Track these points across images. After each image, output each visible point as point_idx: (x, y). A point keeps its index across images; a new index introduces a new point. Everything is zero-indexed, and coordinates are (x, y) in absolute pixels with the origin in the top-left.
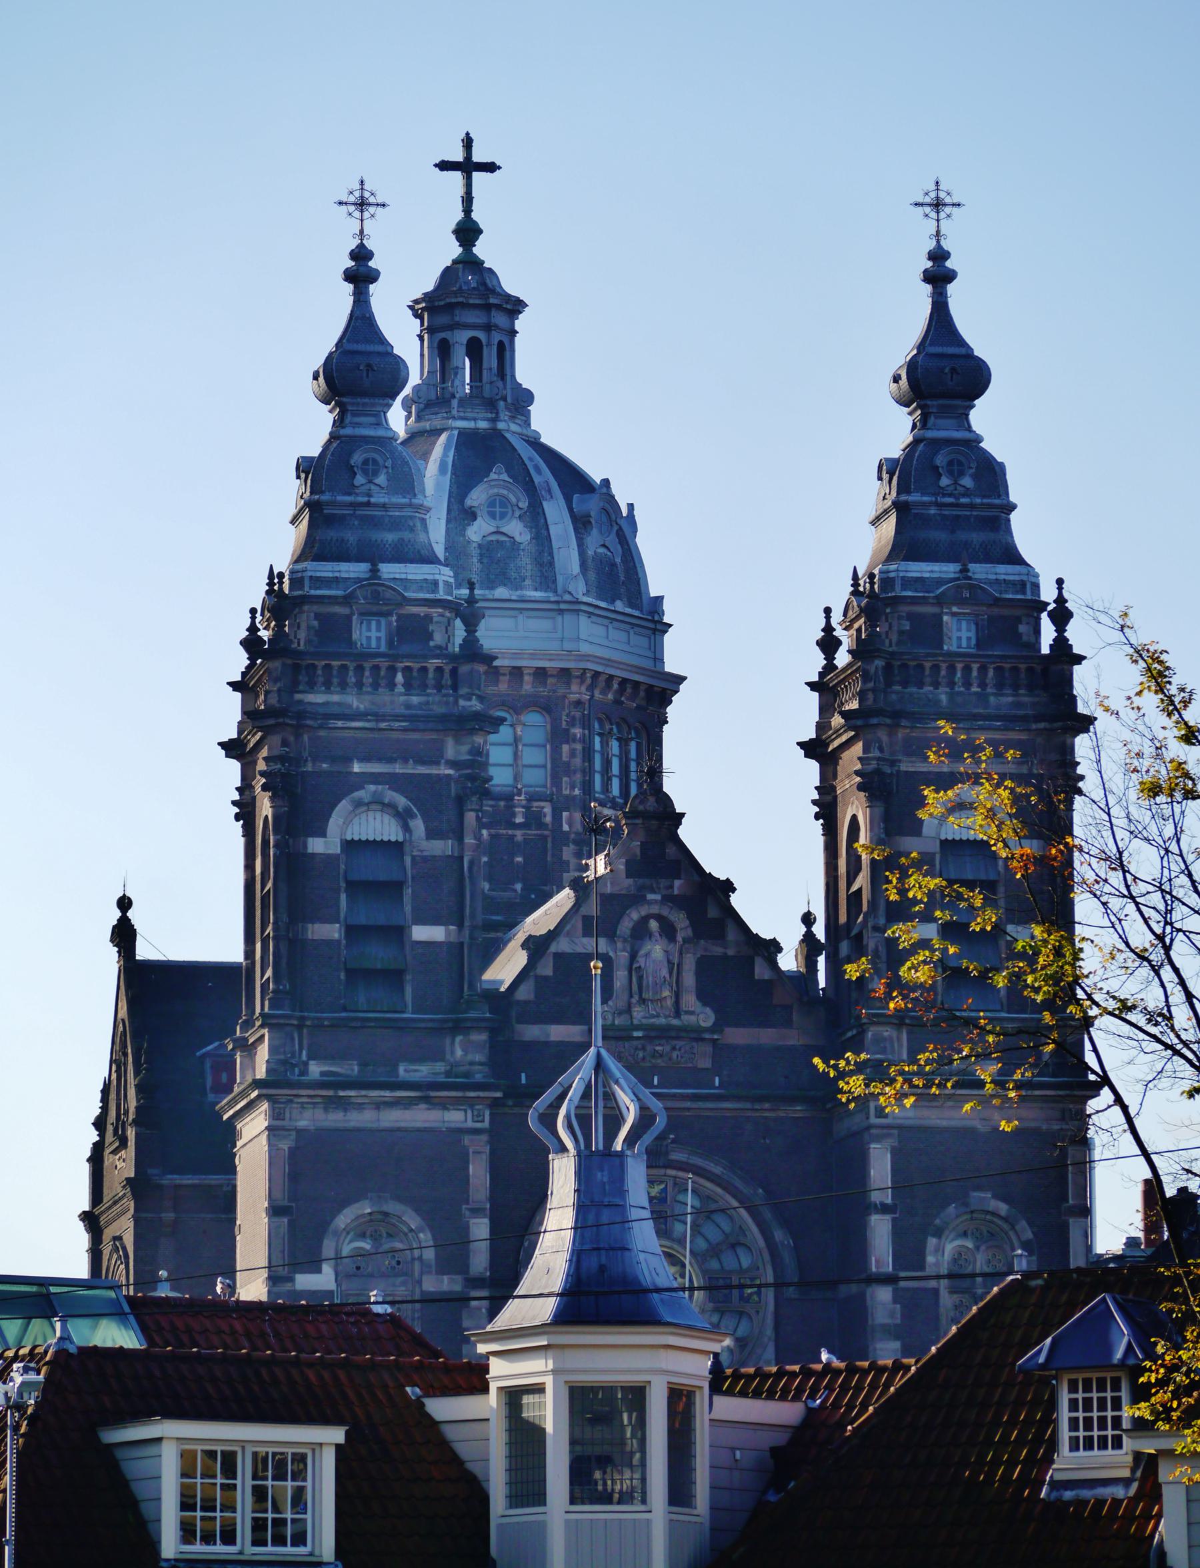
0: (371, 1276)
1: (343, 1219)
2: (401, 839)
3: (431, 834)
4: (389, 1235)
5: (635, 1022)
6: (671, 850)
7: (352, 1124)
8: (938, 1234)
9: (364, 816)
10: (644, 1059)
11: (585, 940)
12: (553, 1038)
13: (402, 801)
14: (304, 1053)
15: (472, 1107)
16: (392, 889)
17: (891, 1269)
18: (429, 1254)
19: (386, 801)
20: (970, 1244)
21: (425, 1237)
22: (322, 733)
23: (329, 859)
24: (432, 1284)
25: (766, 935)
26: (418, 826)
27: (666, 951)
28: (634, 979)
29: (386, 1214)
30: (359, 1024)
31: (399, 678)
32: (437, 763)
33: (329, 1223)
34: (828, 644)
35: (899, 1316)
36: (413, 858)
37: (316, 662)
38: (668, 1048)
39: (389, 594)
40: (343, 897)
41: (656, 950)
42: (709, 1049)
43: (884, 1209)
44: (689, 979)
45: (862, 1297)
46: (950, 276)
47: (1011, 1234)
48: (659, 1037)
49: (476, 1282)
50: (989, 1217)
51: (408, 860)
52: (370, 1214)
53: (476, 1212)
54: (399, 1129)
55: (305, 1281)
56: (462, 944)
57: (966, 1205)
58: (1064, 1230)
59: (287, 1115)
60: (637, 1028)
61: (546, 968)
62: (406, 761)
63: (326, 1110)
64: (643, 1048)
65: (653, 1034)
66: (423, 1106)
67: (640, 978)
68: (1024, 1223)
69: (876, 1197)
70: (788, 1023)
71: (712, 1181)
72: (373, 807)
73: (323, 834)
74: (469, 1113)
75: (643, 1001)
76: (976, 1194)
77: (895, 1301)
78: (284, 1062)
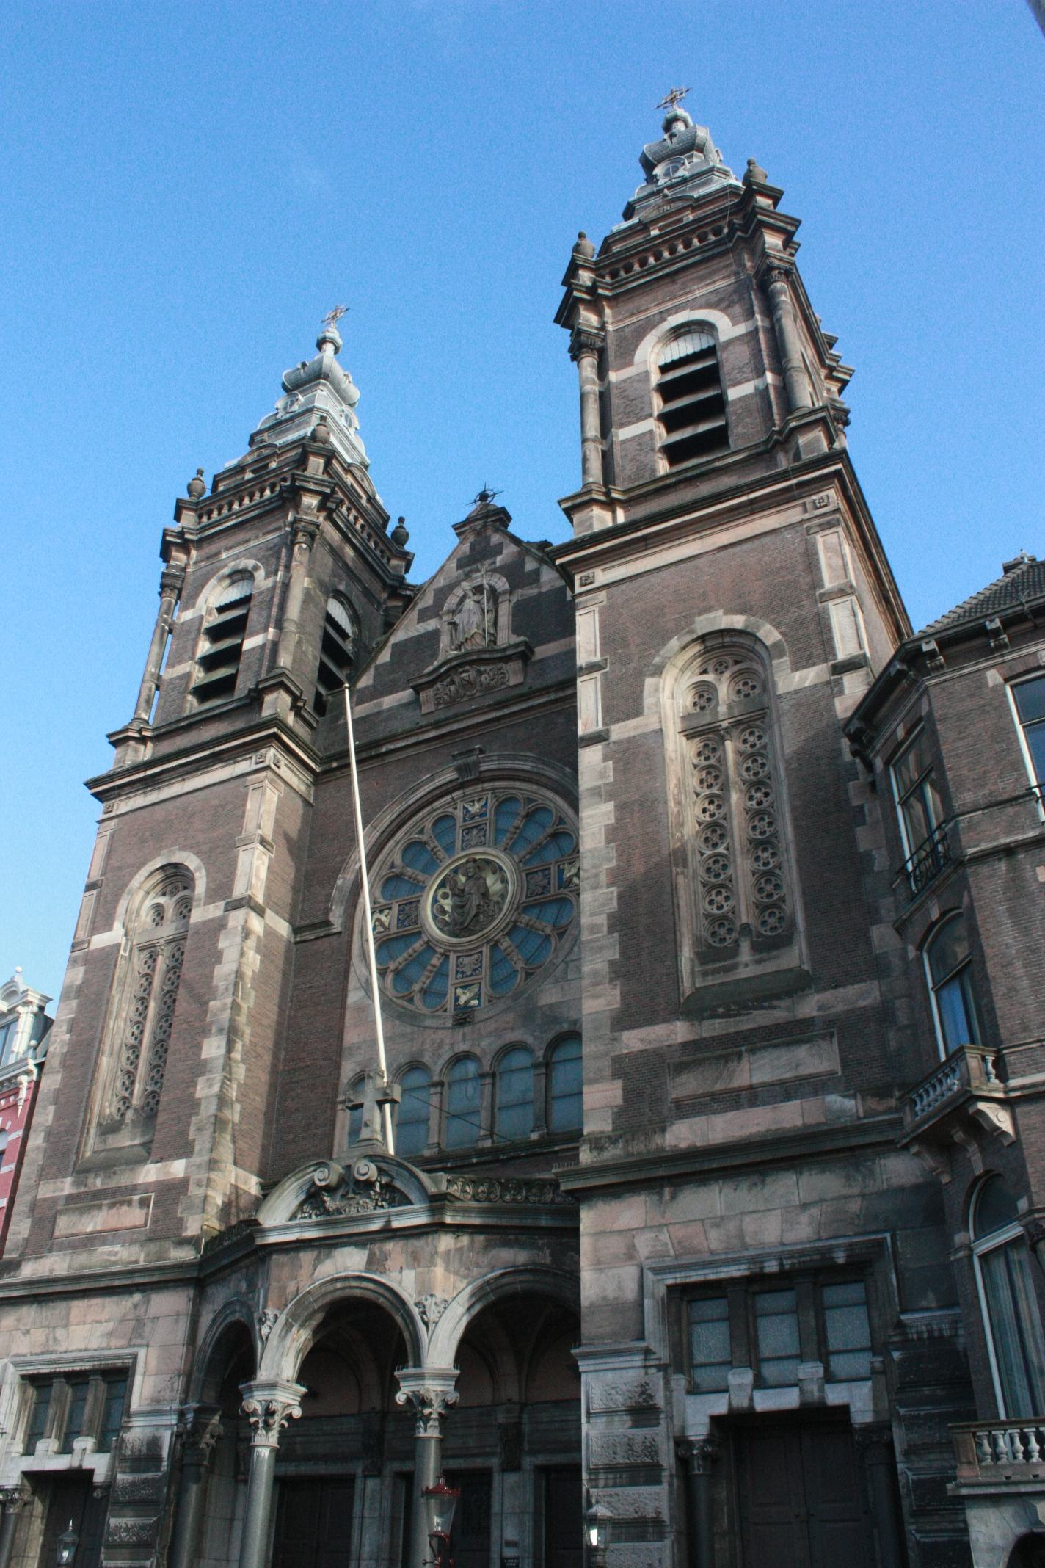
11: (419, 626)
12: (385, 706)
20: (709, 677)
27: (478, 602)
29: (175, 865)
33: (126, 885)
35: (611, 774)
42: (518, 665)
47: (759, 648)
50: (727, 639)
57: (692, 632)
64: (453, 682)
68: (768, 627)
69: (582, 659)
72: (235, 577)
77: (606, 759)
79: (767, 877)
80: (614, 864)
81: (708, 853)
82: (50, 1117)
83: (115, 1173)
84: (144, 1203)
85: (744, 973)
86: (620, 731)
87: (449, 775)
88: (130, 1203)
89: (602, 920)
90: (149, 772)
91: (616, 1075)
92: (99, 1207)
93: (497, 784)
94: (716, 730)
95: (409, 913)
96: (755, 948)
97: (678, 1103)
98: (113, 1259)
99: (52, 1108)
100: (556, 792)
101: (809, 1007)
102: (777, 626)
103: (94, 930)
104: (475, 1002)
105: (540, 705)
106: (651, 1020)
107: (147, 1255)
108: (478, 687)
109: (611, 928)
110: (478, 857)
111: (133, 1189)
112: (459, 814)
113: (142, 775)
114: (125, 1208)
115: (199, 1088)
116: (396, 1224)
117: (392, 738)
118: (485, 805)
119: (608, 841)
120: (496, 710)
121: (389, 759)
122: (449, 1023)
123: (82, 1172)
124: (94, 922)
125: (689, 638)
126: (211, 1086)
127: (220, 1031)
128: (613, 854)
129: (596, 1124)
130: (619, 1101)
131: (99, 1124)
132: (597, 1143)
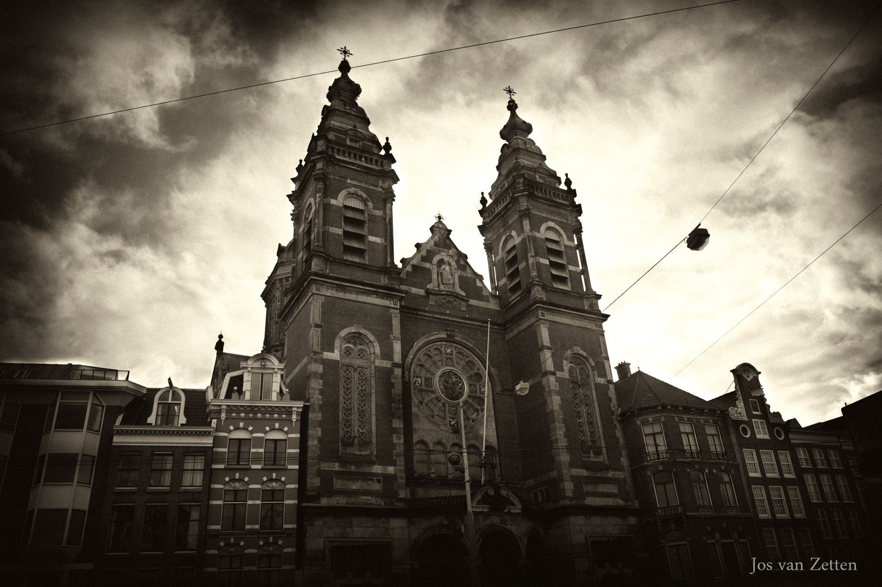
0: (354, 358)
1: (344, 333)
2: (363, 209)
3: (375, 208)
4: (360, 344)
5: (441, 289)
6: (448, 241)
7: (347, 298)
8: (566, 359)
9: (350, 198)
10: (445, 303)
12: (413, 292)
13: (365, 196)
14: (328, 270)
15: (393, 299)
16: (360, 223)
17: (553, 370)
18: (378, 350)
19: (359, 194)
21: (376, 344)
22: (336, 167)
23: (338, 207)
24: (378, 363)
25: (479, 273)
26: (370, 204)
28: (439, 277)
29: (360, 334)
30: (350, 263)
31: (363, 159)
32: (377, 186)
33: (338, 333)
34: (483, 201)
35: (558, 387)
36: (368, 214)
37: (335, 146)
38: (453, 300)
39: (360, 135)
40: (343, 222)
41: (447, 268)
43: (548, 348)
44: (457, 281)
45: (540, 382)
46: (517, 107)
48: (451, 295)
49: (396, 365)
51: (366, 215)
52: (354, 332)
53: (395, 338)
54: (366, 303)
55: (327, 355)
56: (386, 246)
57: (573, 350)
58: (603, 364)
59: (321, 290)
60: (444, 291)
61: (409, 268)
62: (366, 183)
63: (336, 290)
64: (445, 299)
65: (449, 293)
66: (375, 296)
67: (442, 277)
70: (488, 301)
71: (468, 349)
72: (354, 196)
73: (336, 199)
74: (392, 301)
75: (443, 284)
76: (575, 348)
78: (321, 270)
79: (592, 433)
80: (562, 417)
81: (578, 421)
82: (320, 434)
83: (361, 466)
84: (379, 481)
85: (594, 459)
86: (559, 374)
87: (443, 335)
88: (372, 480)
89: (562, 433)
90: (343, 284)
91: (571, 481)
92: (358, 480)
93: (458, 346)
94: (578, 384)
95: (428, 381)
96: (594, 453)
97: (586, 493)
98: (369, 502)
99: (319, 429)
100: (478, 358)
101: (610, 474)
102: (593, 360)
103: (323, 349)
104: (456, 425)
105: (476, 325)
106: (577, 467)
107: (384, 503)
108: (451, 305)
109: (564, 436)
110: (453, 371)
111: (372, 474)
112: (443, 350)
113: (340, 283)
114: (371, 482)
115: (394, 438)
116: (512, 511)
117: (425, 311)
118: (452, 351)
119: (560, 409)
120: (462, 319)
121: (419, 317)
122: (451, 431)
123: (344, 462)
124: (322, 344)
125: (573, 352)
126: (399, 439)
127: (399, 418)
128: (562, 413)
129: (569, 494)
130: (573, 488)
131: (341, 441)
132: (571, 499)
